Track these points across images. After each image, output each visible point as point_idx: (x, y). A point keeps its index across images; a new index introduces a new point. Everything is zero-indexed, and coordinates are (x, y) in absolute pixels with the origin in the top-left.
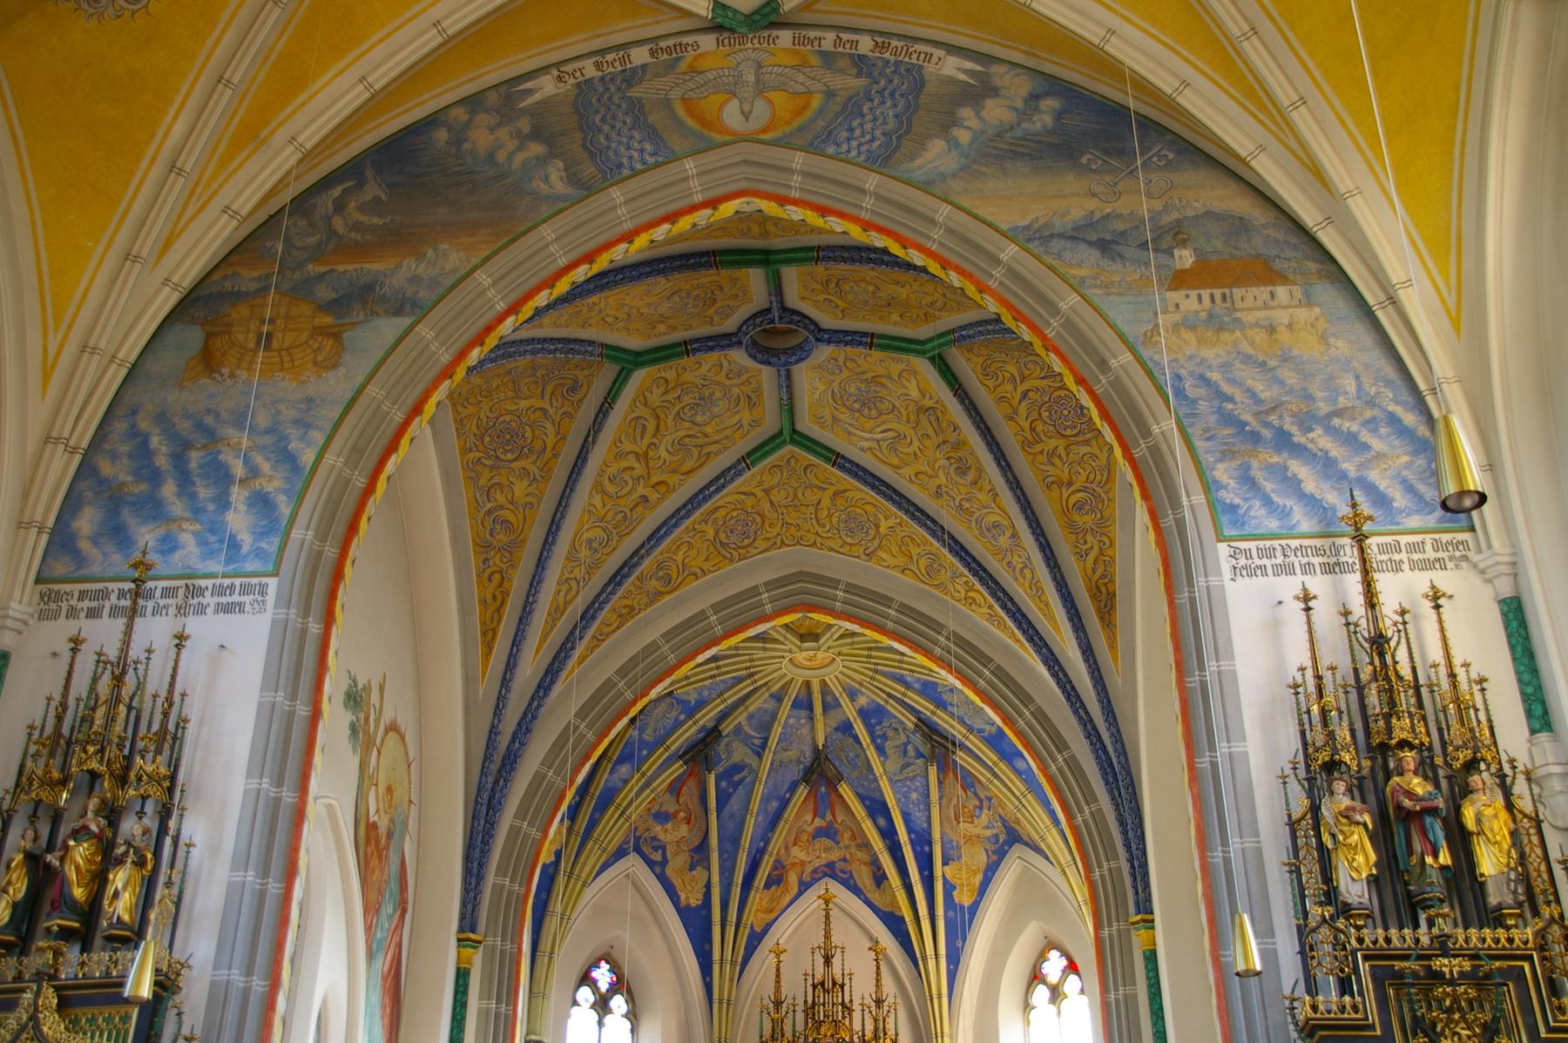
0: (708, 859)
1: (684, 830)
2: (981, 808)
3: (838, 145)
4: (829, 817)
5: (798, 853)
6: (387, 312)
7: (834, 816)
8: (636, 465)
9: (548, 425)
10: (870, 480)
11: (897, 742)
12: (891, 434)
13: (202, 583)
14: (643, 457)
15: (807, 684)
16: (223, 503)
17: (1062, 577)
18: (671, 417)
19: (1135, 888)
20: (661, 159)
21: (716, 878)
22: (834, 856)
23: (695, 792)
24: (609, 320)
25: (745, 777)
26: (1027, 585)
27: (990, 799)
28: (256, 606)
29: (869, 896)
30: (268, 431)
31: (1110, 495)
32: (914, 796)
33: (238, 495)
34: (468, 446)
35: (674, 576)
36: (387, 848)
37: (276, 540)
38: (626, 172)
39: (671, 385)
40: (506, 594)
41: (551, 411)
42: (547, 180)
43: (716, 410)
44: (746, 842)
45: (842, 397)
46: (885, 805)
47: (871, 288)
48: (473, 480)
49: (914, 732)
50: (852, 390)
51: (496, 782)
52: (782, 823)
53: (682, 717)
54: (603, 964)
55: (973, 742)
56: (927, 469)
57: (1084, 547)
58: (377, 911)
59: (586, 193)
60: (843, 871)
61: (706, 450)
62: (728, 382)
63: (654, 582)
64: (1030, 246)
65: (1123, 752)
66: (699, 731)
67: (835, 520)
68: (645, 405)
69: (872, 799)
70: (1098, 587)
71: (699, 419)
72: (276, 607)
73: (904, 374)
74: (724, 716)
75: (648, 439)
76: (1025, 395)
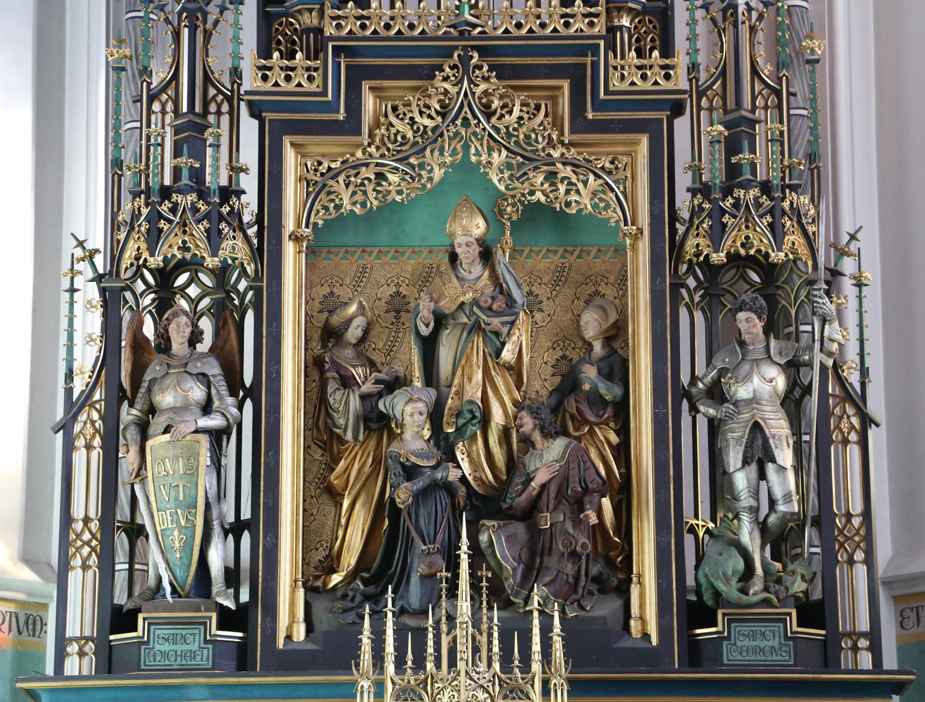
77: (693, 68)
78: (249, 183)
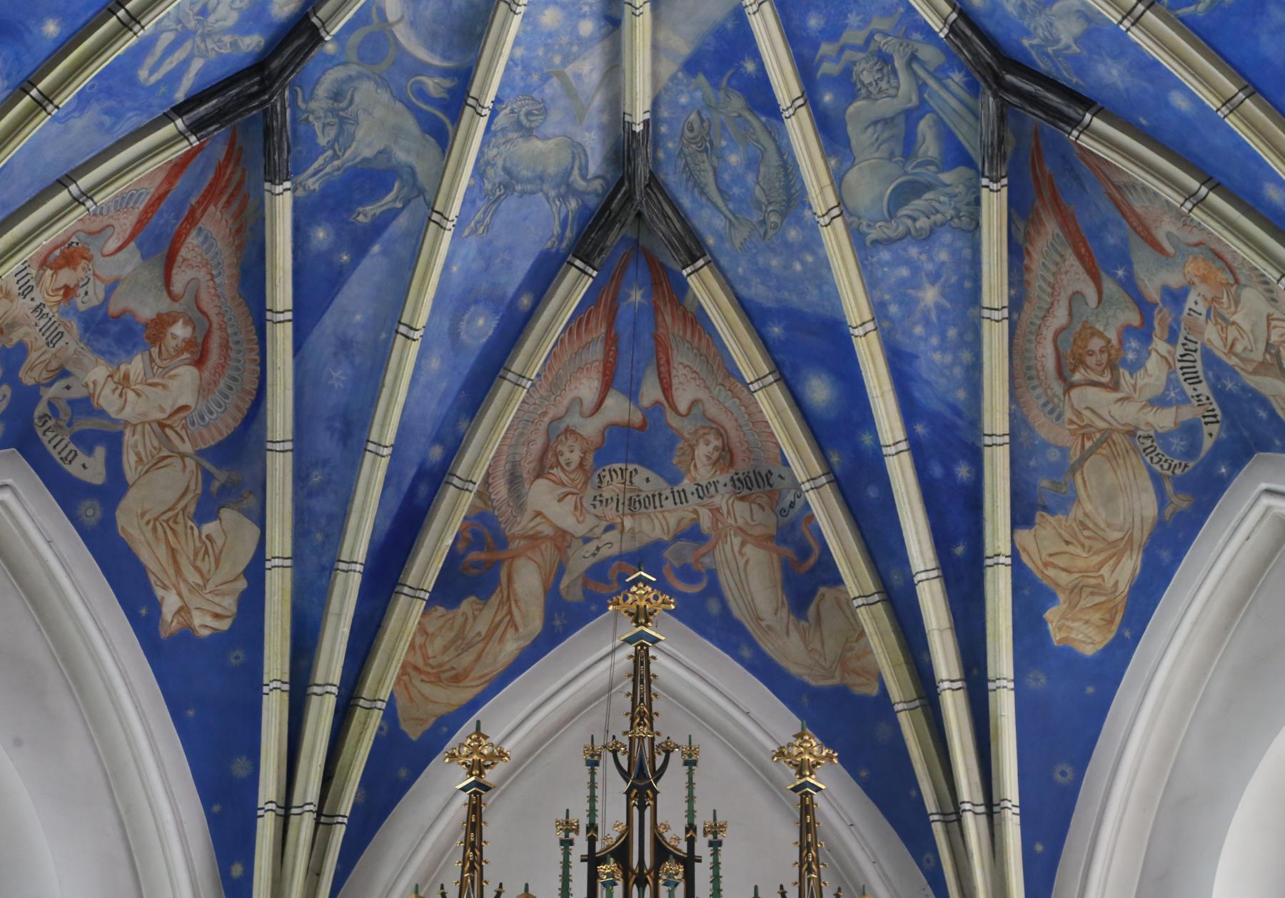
0: (261, 488)
2: (1144, 333)
4: (651, 392)
7: (667, 389)
11: (886, 107)
23: (225, 253)
25: (393, 214)
29: (768, 647)
32: (930, 295)
52: (505, 387)
60: (688, 574)
69: (788, 315)
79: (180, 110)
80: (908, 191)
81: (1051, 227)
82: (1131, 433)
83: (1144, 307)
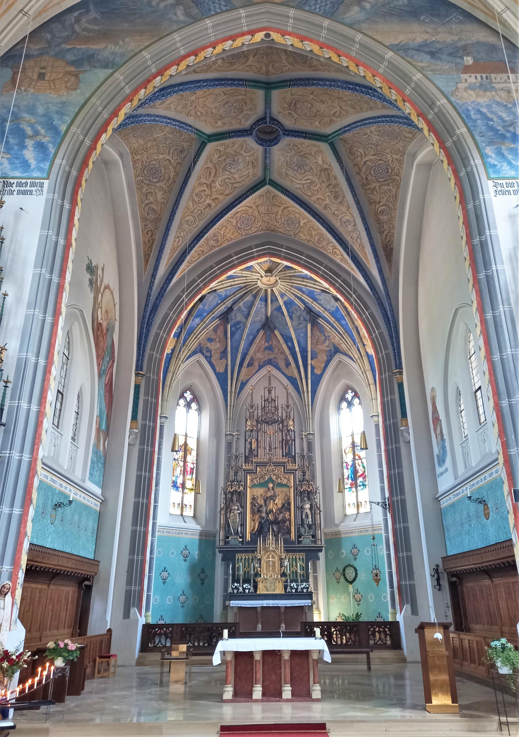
1: (218, 345)
2: (326, 340)
3: (310, 6)
4: (270, 343)
5: (259, 355)
6: (101, 67)
8: (207, 189)
9: (171, 167)
10: (299, 202)
11: (297, 315)
12: (309, 181)
13: (12, 181)
14: (209, 186)
15: (266, 291)
16: (23, 146)
17: (373, 241)
18: (221, 169)
19: (395, 360)
20: (228, 8)
21: (229, 363)
22: (271, 357)
24: (199, 113)
25: (241, 327)
26: (358, 245)
27: (329, 336)
28: (38, 192)
30: (43, 116)
31: (395, 207)
32: (302, 335)
33: (29, 143)
34: (137, 173)
35: (220, 240)
36: (106, 335)
37: (48, 164)
38: (212, 13)
39: (222, 154)
40: (154, 240)
41: (172, 161)
42: (176, 14)
43: (239, 167)
44: (241, 350)
45: (290, 164)
46: (291, 338)
47: (309, 106)
48: (140, 189)
49: (303, 312)
50: (295, 160)
51: (150, 315)
53: (219, 301)
54: (188, 392)
55: (326, 315)
56: (322, 197)
57: (382, 229)
58: (103, 358)
59: (193, 20)
60: (275, 362)
61: (235, 185)
62: (245, 154)
63: (212, 242)
64: (399, 52)
65: (392, 310)
66: (225, 308)
67: (283, 220)
68: (211, 162)
70: (387, 246)
71: (232, 171)
72: (48, 193)
73: (317, 153)
74: (234, 303)
75: (211, 179)
76: (365, 163)
77: (298, 465)
78: (243, 480)
79: (218, 318)
80: (299, 324)
81: (316, 328)
82: (324, 350)
83: (326, 337)
